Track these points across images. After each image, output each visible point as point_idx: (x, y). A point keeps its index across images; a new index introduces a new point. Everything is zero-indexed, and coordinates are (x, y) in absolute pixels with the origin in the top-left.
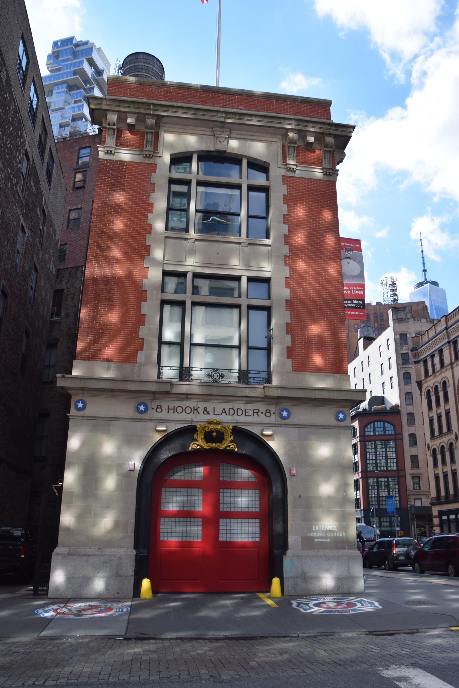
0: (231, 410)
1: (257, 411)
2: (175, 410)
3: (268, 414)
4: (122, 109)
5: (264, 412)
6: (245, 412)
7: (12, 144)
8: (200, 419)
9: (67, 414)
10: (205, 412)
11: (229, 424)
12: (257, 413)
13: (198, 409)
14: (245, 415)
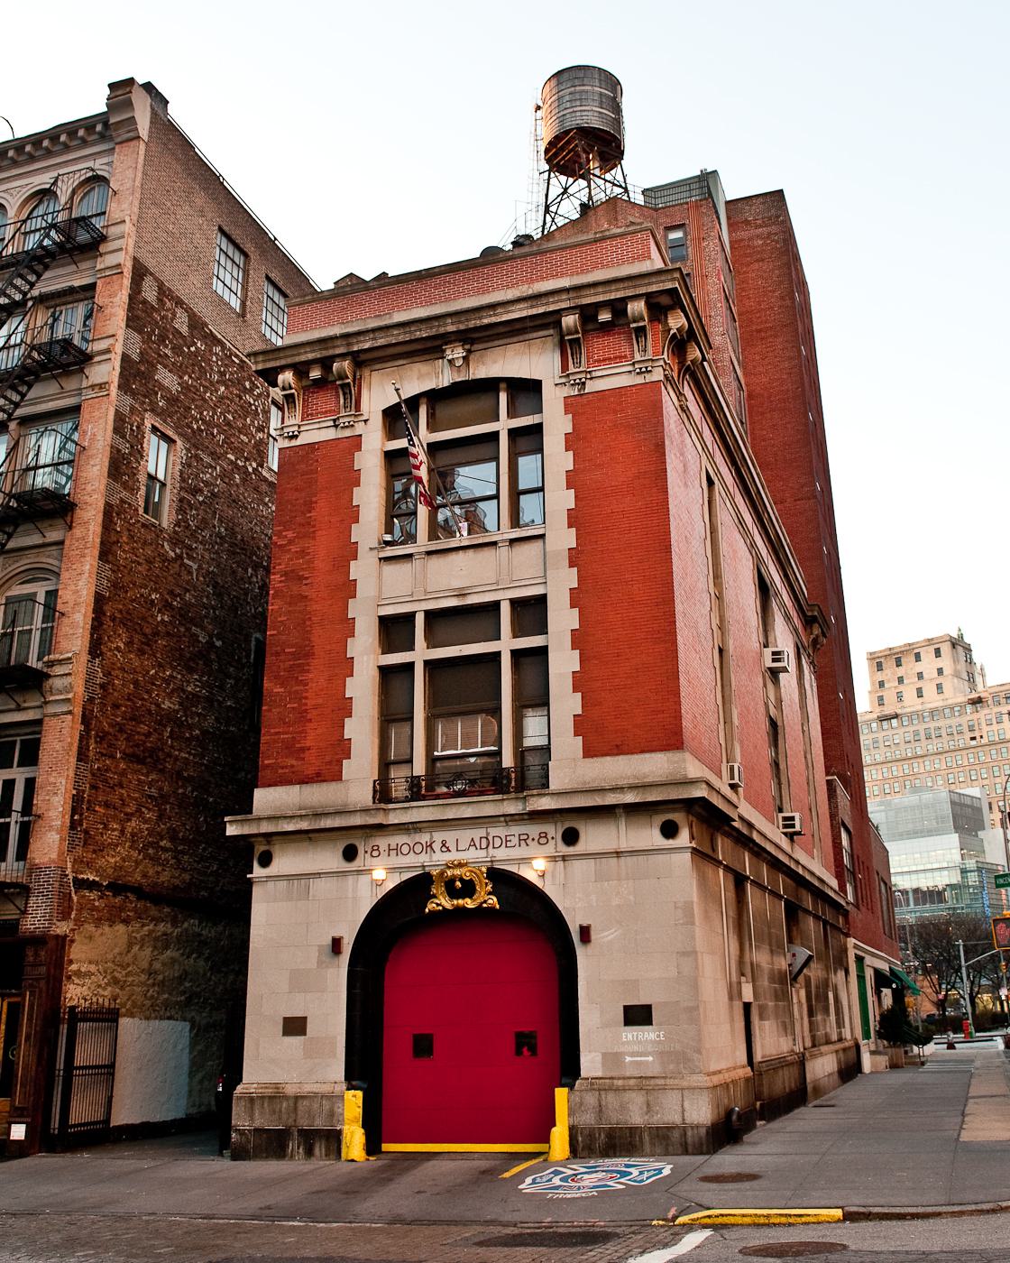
0: (484, 841)
1: (525, 837)
2: (398, 850)
3: (543, 841)
4: (297, 359)
5: (536, 839)
6: (506, 841)
7: (229, 412)
8: (435, 860)
9: (248, 876)
10: (444, 849)
11: (480, 865)
12: (525, 840)
13: (433, 845)
14: (506, 847)
